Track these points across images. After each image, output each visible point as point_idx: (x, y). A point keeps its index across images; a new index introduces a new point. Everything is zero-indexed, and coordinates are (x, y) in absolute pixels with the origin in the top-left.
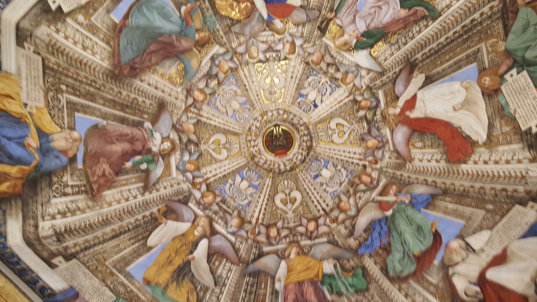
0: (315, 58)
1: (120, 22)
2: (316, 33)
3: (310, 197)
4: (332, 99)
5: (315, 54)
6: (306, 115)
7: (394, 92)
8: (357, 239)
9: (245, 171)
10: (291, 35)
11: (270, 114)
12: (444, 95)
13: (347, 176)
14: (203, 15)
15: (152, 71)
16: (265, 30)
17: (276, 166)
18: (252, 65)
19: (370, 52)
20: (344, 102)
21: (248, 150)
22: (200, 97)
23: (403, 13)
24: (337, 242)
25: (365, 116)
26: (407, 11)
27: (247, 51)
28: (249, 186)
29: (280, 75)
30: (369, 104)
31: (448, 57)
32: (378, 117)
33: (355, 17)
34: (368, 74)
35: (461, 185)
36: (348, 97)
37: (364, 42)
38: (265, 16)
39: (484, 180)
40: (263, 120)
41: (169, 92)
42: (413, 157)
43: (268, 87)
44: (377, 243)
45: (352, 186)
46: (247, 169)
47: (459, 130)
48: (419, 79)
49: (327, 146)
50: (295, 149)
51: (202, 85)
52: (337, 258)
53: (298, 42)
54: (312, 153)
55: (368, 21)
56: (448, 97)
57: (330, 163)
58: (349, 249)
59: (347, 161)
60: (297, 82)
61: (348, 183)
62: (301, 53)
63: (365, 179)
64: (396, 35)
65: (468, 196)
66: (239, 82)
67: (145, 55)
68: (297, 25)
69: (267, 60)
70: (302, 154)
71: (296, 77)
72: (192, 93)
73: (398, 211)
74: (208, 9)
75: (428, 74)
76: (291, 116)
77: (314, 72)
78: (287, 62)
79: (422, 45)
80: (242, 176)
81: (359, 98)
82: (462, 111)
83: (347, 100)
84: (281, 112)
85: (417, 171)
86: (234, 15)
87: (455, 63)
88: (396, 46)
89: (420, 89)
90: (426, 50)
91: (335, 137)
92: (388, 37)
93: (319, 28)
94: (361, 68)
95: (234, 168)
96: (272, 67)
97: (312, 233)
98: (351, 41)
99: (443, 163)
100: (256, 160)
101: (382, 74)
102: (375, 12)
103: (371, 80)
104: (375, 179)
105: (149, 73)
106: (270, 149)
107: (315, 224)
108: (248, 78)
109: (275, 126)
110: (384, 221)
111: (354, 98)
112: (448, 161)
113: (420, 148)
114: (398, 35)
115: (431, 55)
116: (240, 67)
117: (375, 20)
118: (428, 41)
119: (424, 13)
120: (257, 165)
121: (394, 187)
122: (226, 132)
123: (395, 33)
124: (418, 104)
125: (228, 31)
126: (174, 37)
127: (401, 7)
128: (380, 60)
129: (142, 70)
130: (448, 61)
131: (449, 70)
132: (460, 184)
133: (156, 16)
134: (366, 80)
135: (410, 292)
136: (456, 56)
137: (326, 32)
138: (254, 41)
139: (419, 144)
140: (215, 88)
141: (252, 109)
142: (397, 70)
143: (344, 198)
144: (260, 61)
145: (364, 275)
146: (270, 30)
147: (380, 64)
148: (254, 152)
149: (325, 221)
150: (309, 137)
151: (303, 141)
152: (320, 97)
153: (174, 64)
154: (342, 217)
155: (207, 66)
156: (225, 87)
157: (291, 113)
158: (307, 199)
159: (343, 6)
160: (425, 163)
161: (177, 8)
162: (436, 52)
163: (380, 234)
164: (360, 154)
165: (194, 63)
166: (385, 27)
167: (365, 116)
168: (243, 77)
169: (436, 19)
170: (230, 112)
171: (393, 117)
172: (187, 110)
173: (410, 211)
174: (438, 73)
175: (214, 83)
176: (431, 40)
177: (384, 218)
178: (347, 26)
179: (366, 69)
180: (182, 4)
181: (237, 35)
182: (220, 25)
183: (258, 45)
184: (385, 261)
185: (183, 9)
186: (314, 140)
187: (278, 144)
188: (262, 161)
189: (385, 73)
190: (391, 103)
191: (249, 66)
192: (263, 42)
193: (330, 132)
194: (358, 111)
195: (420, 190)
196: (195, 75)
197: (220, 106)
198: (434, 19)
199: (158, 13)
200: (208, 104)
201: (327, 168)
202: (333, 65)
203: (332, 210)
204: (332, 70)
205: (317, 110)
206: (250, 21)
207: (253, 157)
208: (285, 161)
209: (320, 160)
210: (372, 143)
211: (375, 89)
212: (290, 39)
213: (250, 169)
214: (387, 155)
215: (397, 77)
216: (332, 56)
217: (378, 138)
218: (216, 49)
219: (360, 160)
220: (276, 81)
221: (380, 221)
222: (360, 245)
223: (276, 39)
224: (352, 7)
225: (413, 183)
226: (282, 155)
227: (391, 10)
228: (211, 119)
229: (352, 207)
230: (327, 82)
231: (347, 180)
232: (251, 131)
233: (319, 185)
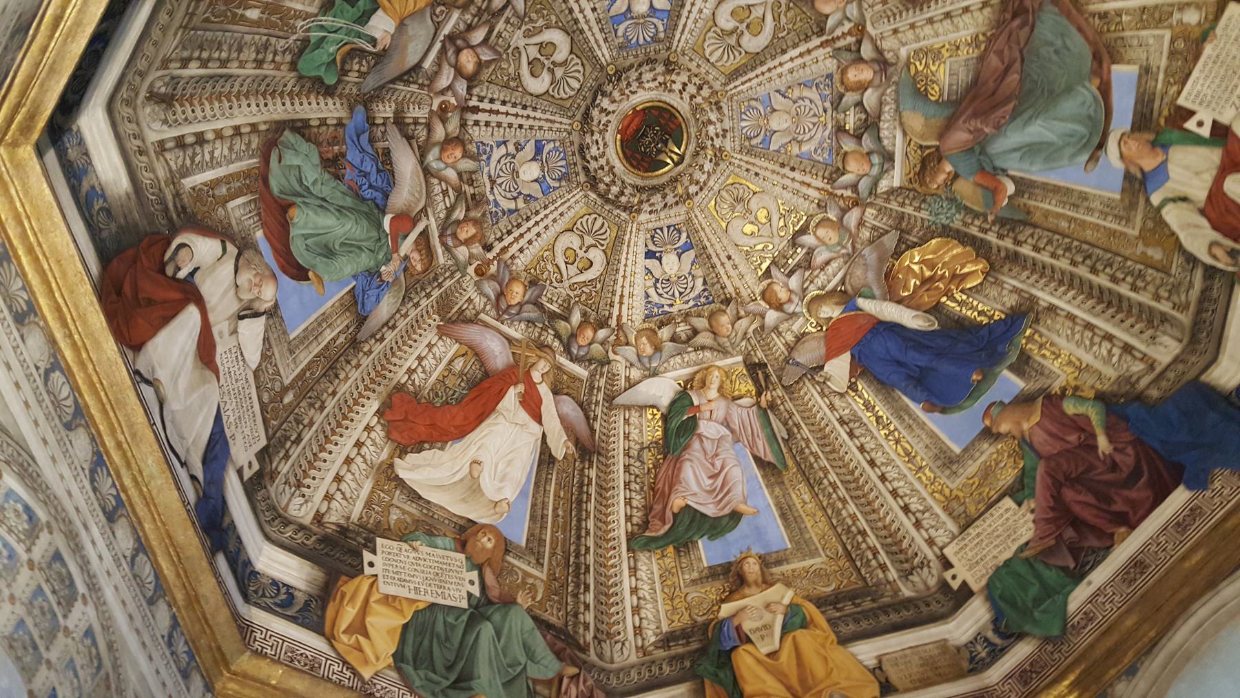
0: (725, 320)
1: (1109, 72)
2: (760, 354)
3: (514, 105)
4: (639, 291)
5: (730, 326)
6: (651, 226)
7: (566, 394)
8: (384, 124)
9: (661, 28)
10: (794, 315)
11: (708, 167)
12: (509, 463)
13: (497, 204)
14: (966, 208)
15: (981, 37)
16: (843, 282)
17: (616, 94)
18: (811, 212)
19: (658, 410)
20: (617, 306)
21: (689, 70)
22: (854, 75)
23: (677, 503)
24: (408, 83)
25: (567, 319)
26: (676, 510)
27: (840, 225)
28: (629, 9)
29: (753, 241)
30: (582, 341)
31: (560, 513)
32: (549, 338)
33: (732, 431)
34: (628, 379)
35: (347, 378)
36: (619, 317)
37: (683, 416)
38: (861, 302)
39: (332, 420)
40: (709, 146)
41: (917, 31)
42: (444, 338)
43: (753, 205)
44: (353, 156)
45: (474, 196)
46: (662, 35)
47: (439, 445)
48: (560, 446)
49: (571, 213)
50: (613, 155)
51: (870, 98)
52: (381, 57)
53: (772, 316)
54: (582, 178)
55: (708, 445)
56: (500, 467)
57: (540, 195)
58: (377, 95)
59: (519, 226)
60: (715, 259)
61: (484, 195)
62: (751, 307)
63: (467, 231)
64: (651, 466)
65: (324, 374)
66: (807, 164)
67: (1017, 54)
68: (800, 338)
69: (794, 243)
70: (596, 159)
71: (722, 264)
72: (877, 67)
73: (380, 239)
74: (965, 224)
75: (557, 464)
76: (670, 199)
77: (703, 300)
78: (760, 273)
79: (607, 490)
80: (658, 14)
81: (602, 333)
82: (466, 470)
83: (616, 312)
84: (693, 189)
85: (417, 322)
86: (912, 257)
87: (544, 516)
88: (636, 453)
89: (544, 436)
90: (593, 490)
91: (573, 241)
92: (660, 454)
93: (763, 366)
94: (645, 377)
95: (685, 13)
96: (776, 240)
97: (458, 51)
98: (699, 396)
99: (401, 376)
100: (660, 68)
101: (610, 398)
102: (713, 465)
103: (614, 375)
104: (455, 247)
105: (983, 29)
106: (653, 111)
107: (464, 70)
108: (797, 185)
109: (682, 158)
110: (379, 201)
111: (609, 326)
112: (399, 388)
113: (451, 361)
114: (649, 469)
115: (581, 493)
116: (828, 187)
117: (700, 455)
118: (604, 502)
119: (651, 531)
120: (651, 61)
121: (419, 267)
122: (756, 60)
123: (655, 467)
124: (523, 416)
125: (901, 224)
126: (987, 130)
127: (687, 506)
128: (635, 414)
129: (999, 25)
130: (555, 509)
131: (540, 500)
132: (352, 378)
133: (1050, 136)
134: (620, 367)
135: (239, 145)
136: (553, 526)
137: (748, 371)
138: (844, 251)
139: (458, 365)
140: (843, 115)
141: (747, 143)
142: (597, 426)
143: (467, 165)
144: (804, 231)
145: (318, 80)
146: (834, 290)
147: (628, 408)
148: (674, 77)
149: (455, 95)
150: (610, 196)
151: (613, 182)
152: (657, 274)
153: (950, 85)
154: (439, 133)
155: (888, 138)
156: (823, 134)
157: (677, 203)
158: (516, 97)
159: (763, 427)
160: (421, 349)
161: (1022, 178)
162: (580, 502)
163: (366, 175)
164: (513, 257)
165: (916, 121)
166: (678, 461)
167: (567, 319)
168: (807, 179)
169: (628, 540)
170: (778, 101)
171: (531, 360)
172: (860, 30)
173: (365, 261)
174: (547, 481)
175: (851, 122)
176: (603, 509)
177: (386, 205)
178: (728, 408)
179: (640, 381)
180: (1019, 193)
181: (879, 234)
182: (922, 219)
183: (831, 251)
184: (318, 144)
185: (1011, 188)
186: (599, 201)
187: (651, 134)
188: (647, 76)
189: (606, 405)
190: (555, 376)
191: (815, 206)
192: (828, 263)
193: (589, 240)
194: (584, 314)
195: (385, 307)
196: (897, 101)
197: (806, 93)
198: (631, 537)
199: (1050, 144)
200: (830, 76)
201: (536, 181)
202: (689, 339)
203: (463, 124)
204: (682, 329)
205: (641, 250)
206: (878, 274)
207: (670, 67)
208: (609, 118)
209: (559, 180)
210: (517, 293)
211: (596, 369)
212: (790, 308)
213: (655, 39)
214: (479, 301)
215: (587, 418)
216: (703, 348)
217: (517, 308)
218: (896, 178)
219: (504, 250)
220: (749, 228)
221: (386, 196)
222: (371, 121)
223: (812, 287)
224: (750, 438)
225: (403, 303)
226: (626, 123)
227: (695, 488)
228: (801, 55)
229: (443, 166)
230: (671, 305)
231: (491, 198)
232: (714, 107)
233: (522, 141)
